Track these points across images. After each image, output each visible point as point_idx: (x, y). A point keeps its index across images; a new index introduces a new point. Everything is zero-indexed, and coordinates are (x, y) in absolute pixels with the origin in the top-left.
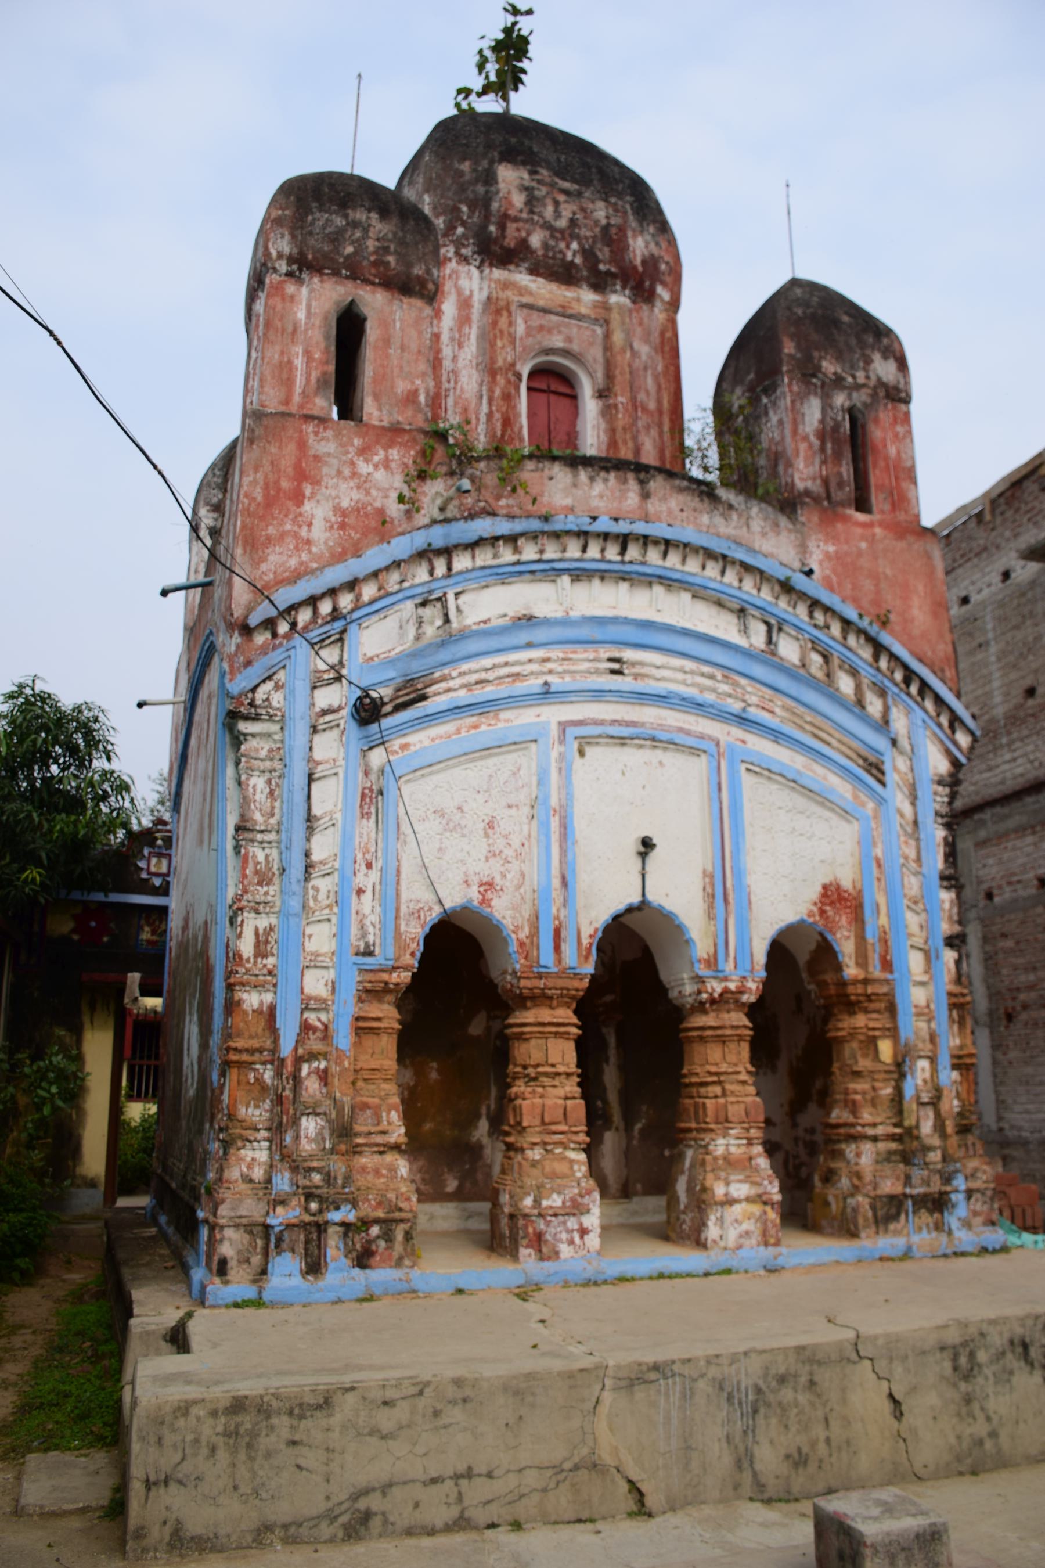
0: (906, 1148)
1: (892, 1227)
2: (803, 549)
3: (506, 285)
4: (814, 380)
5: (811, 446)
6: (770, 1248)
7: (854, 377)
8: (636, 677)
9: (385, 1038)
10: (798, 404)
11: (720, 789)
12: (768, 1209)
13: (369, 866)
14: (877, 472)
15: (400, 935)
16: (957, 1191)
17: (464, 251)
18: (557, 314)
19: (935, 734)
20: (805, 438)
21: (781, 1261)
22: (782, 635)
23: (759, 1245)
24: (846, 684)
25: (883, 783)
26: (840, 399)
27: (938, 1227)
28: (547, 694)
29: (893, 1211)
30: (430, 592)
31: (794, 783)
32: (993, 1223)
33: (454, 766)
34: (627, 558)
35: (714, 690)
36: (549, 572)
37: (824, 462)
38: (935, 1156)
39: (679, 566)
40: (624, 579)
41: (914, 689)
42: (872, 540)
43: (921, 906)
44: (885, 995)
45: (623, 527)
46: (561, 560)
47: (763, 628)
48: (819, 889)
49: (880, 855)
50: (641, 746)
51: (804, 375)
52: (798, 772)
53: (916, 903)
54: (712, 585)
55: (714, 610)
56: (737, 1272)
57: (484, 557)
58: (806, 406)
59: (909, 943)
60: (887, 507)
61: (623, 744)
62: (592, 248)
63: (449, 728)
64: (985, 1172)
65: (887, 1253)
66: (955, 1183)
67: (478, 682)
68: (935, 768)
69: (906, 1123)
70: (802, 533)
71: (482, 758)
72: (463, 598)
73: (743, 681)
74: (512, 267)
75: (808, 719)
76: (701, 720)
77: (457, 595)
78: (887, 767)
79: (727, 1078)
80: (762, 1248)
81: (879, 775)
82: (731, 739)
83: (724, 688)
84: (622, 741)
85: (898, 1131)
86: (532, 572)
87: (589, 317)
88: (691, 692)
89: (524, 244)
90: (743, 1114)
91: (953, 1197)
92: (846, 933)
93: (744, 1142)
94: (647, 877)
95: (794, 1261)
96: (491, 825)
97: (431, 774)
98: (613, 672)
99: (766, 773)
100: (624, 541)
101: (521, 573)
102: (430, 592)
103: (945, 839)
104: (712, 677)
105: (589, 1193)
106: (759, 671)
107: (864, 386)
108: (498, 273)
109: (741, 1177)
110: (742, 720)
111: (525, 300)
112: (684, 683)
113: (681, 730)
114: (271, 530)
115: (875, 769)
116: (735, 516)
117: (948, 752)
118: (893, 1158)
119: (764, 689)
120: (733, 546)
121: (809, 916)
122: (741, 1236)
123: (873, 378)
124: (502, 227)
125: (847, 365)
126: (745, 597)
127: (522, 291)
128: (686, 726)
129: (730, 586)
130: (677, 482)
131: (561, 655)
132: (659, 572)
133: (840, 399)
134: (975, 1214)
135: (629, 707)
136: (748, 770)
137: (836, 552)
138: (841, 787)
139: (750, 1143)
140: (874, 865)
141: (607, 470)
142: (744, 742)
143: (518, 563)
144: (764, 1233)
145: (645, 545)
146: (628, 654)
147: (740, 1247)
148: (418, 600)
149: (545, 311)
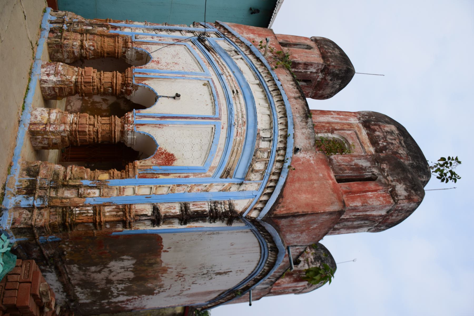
0: (59, 183)
1: (25, 172)
2: (306, 150)
3: (358, 127)
4: (376, 164)
5: (350, 161)
6: (28, 125)
7: (388, 175)
8: (234, 97)
9: (113, 44)
10: (363, 158)
11: (203, 118)
12: (44, 126)
13: (160, 40)
14: (356, 185)
15: (141, 44)
16: (34, 200)
17: (361, 118)
18: (360, 141)
19: (252, 202)
20: (352, 160)
21: (22, 126)
22: (269, 143)
23: (31, 121)
24: (259, 166)
25: (221, 177)
26: (376, 171)
27: (19, 192)
28: (220, 76)
29: (32, 173)
30: (239, 52)
31: (212, 142)
32: (13, 224)
33: (192, 57)
34: (271, 92)
35: (238, 117)
36: (258, 76)
37: (347, 165)
38: (53, 194)
39: (276, 106)
40: (265, 96)
41: (268, 191)
42: (324, 178)
43: (170, 192)
44: (129, 175)
45: (280, 88)
46: (262, 77)
47: (269, 136)
48: (171, 153)
49: (190, 177)
50: (211, 99)
51: (376, 159)
52: (217, 145)
53: (171, 190)
54: (275, 116)
55: (268, 122)
56: (22, 111)
57: (254, 61)
58: (364, 160)
59: (152, 186)
60: (344, 189)
61: (210, 95)
62: (388, 148)
63: (202, 57)
64: (41, 220)
65: (13, 168)
66: (39, 200)
67: (217, 61)
68: (237, 205)
69: (70, 181)
70: (311, 149)
71: (196, 62)
72: (241, 60)
73: (245, 128)
74: (365, 129)
75: (239, 149)
76: (226, 116)
77: (241, 58)
78: (229, 179)
79: (95, 125)
80: (29, 122)
81: (224, 176)
82: (222, 124)
83: (240, 122)
84: (211, 94)
85: (68, 178)
86: (256, 73)
87: (365, 150)
88: (235, 112)
89: (374, 131)
90: (82, 123)
91: (32, 198)
92: (154, 162)
93: (71, 122)
94: (167, 98)
95: (21, 131)
96: (176, 63)
97: (188, 53)
98: (233, 92)
99: (213, 134)
100: (277, 89)
101: (255, 71)
102: (239, 52)
103: (205, 211)
104: (242, 117)
105: (61, 77)
106: (251, 131)
107: (388, 180)
108: (361, 125)
109: (58, 117)
110: (230, 126)
111: (357, 132)
112: (237, 109)
113: (220, 110)
114: (242, 29)
115: (227, 174)
116: (304, 124)
117: (246, 209)
118: (55, 176)
119: (245, 134)
120: (291, 118)
121: (160, 148)
122: (36, 115)
123: (394, 183)
124: (375, 125)
125: (391, 173)
126: (276, 126)
127: (360, 130)
128: (222, 112)
129: (278, 121)
130: (305, 107)
131: (234, 80)
132: (272, 102)
133: (376, 171)
134: (21, 214)
135: (223, 94)
136: (212, 128)
137: (312, 164)
138: (216, 161)
139: (71, 124)
140: (186, 175)
141: (297, 88)
142: (223, 128)
143: (257, 68)
144: (35, 124)
145: (278, 95)
146: (241, 96)
147: (32, 115)
148: (236, 50)
149: (358, 138)
